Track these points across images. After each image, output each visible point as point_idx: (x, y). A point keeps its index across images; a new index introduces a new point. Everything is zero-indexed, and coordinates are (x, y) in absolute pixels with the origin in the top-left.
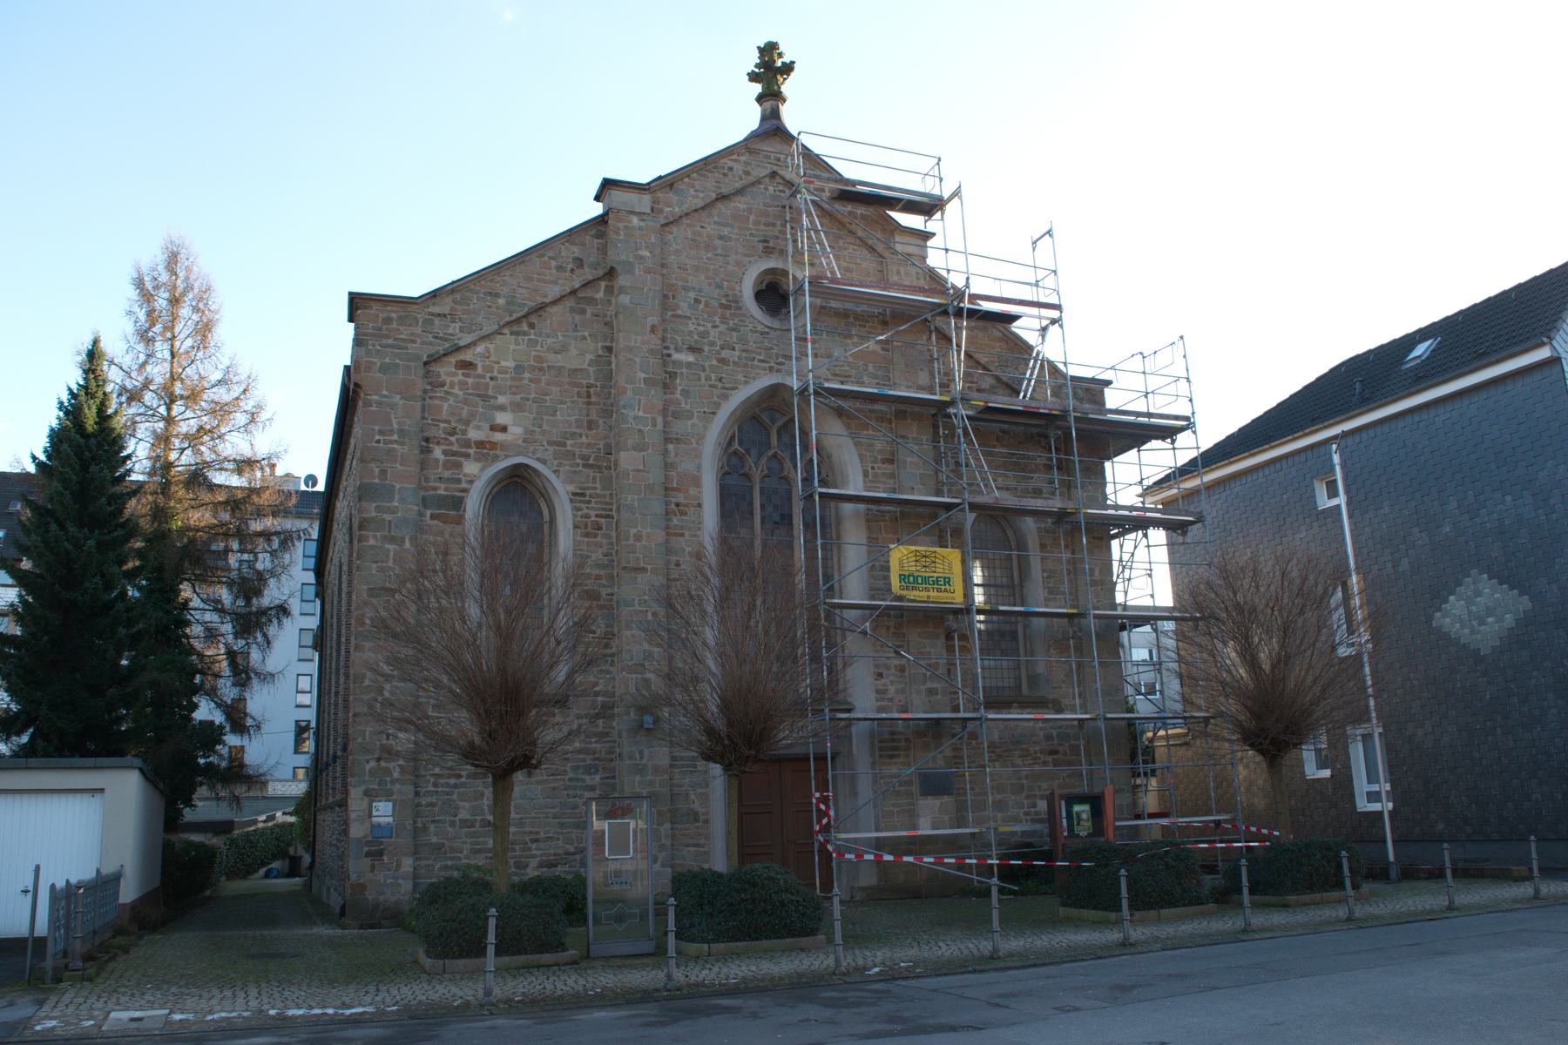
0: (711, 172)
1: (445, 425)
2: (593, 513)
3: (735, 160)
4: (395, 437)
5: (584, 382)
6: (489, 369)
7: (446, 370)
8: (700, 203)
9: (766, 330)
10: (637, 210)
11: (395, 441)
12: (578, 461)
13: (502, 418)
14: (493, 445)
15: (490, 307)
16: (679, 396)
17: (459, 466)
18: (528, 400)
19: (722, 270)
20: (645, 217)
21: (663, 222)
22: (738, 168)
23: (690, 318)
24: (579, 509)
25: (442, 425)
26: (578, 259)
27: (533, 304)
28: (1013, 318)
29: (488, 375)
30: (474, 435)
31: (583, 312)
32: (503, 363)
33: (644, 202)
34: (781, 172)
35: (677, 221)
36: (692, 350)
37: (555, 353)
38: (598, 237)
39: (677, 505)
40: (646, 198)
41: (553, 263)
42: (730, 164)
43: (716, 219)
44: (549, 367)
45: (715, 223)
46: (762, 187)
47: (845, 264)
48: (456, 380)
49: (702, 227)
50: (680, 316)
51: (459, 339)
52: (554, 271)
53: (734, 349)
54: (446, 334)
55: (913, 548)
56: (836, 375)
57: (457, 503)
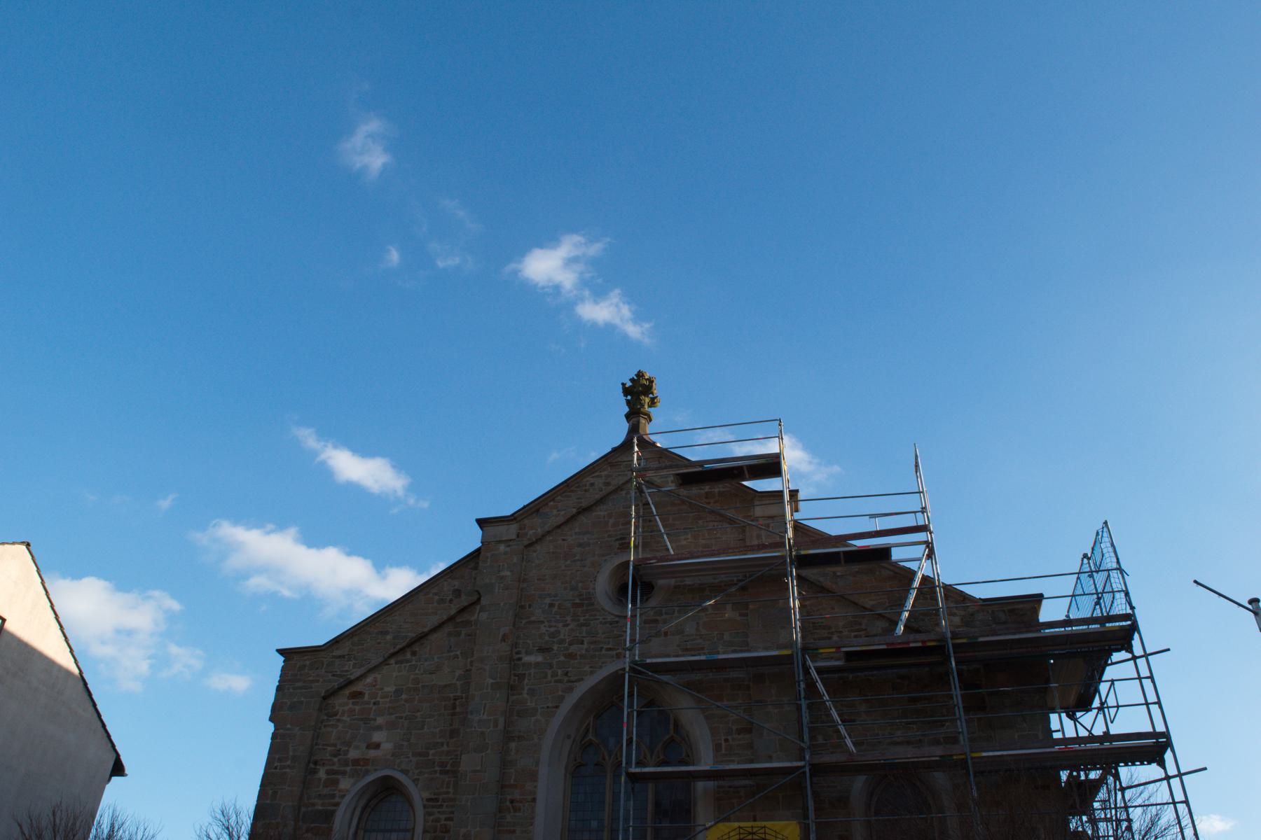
0: (572, 491)
1: (333, 748)
2: (443, 817)
3: (597, 476)
4: (289, 763)
5: (451, 695)
7: (342, 703)
8: (562, 520)
9: (617, 619)
10: (504, 539)
11: (289, 766)
12: (437, 768)
13: (377, 737)
14: (366, 761)
15: (379, 643)
16: (525, 696)
17: (336, 782)
18: (401, 718)
19: (579, 573)
20: (511, 543)
21: (526, 542)
23: (543, 622)
24: (430, 814)
25: (329, 749)
26: (457, 590)
27: (414, 635)
28: (885, 552)
29: (373, 700)
30: (353, 754)
32: (387, 689)
33: (511, 531)
35: (540, 539)
36: (542, 650)
37: (430, 673)
39: (512, 801)
40: (513, 529)
42: (592, 480)
43: (577, 530)
44: (423, 686)
45: (576, 533)
46: (624, 492)
47: (703, 542)
48: (346, 708)
49: (564, 540)
50: (534, 622)
51: (351, 674)
52: (435, 604)
53: (582, 643)
54: (342, 671)
55: (736, 825)
56: (687, 650)
57: (328, 816)
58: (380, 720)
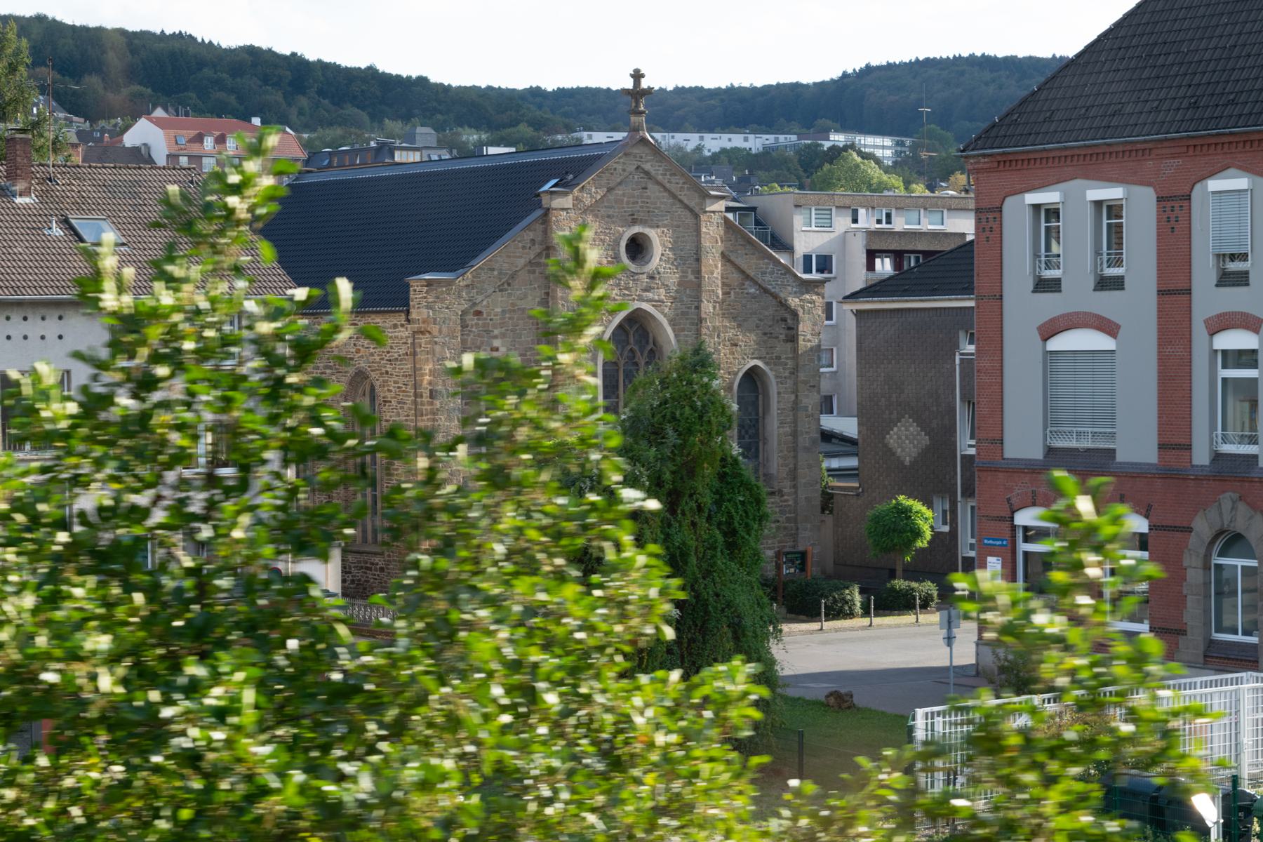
3: (618, 163)
6: (489, 314)
13: (496, 343)
22: (619, 167)
27: (510, 272)
31: (534, 272)
34: (643, 166)
38: (542, 224)
41: (520, 245)
58: (496, 332)
